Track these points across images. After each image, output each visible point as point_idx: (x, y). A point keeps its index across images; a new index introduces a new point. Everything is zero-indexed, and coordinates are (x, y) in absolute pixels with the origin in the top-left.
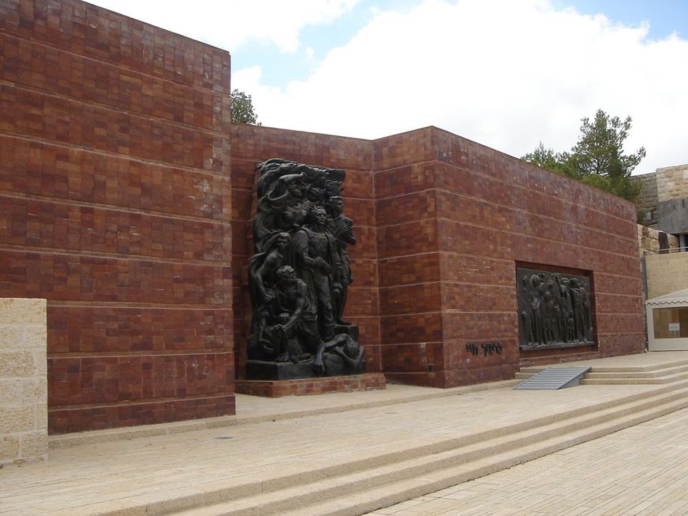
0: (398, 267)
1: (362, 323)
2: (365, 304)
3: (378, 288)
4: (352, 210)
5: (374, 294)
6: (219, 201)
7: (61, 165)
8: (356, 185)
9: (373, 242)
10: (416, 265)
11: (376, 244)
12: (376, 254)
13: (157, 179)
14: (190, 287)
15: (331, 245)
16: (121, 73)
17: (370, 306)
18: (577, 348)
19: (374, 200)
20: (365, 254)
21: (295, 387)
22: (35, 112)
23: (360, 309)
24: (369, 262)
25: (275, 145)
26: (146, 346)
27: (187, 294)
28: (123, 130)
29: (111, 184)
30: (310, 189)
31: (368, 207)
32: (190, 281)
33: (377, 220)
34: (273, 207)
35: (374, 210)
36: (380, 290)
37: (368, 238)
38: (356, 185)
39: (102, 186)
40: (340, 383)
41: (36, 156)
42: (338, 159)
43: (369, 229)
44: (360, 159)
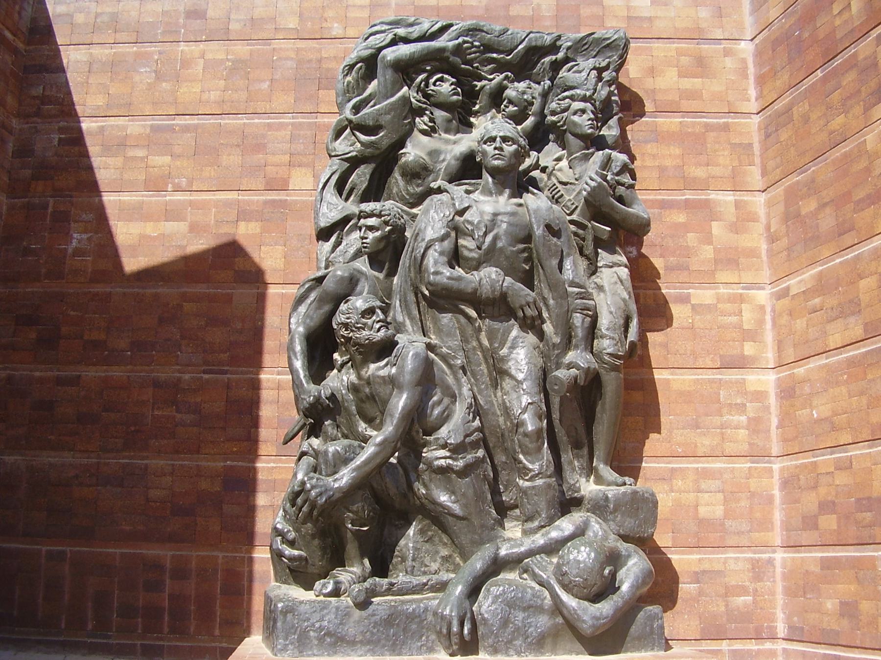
0: (817, 301)
1: (714, 484)
2: (722, 427)
3: (771, 378)
4: (678, 151)
5: (760, 396)
8: (688, 83)
9: (755, 239)
10: (863, 283)
11: (764, 247)
12: (765, 275)
15: (539, 231)
17: (743, 433)
19: (756, 119)
20: (723, 276)
23: (705, 443)
24: (741, 299)
30: (501, 89)
31: (737, 141)
33: (764, 173)
34: (363, 137)
35: (757, 148)
36: (779, 382)
37: (736, 228)
38: (688, 83)
42: (629, 18)
43: (738, 204)
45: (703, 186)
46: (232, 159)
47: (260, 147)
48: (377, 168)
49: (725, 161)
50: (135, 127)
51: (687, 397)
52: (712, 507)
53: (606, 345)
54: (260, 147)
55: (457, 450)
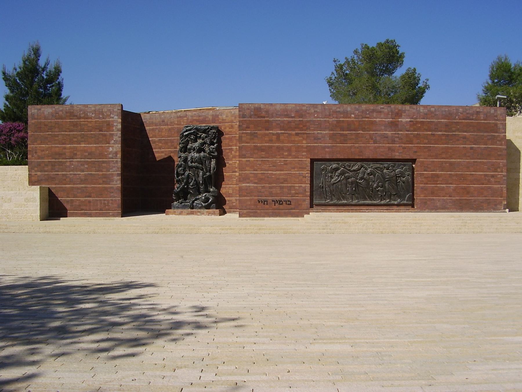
6: (116, 153)
7: (64, 151)
8: (230, 130)
13: (93, 150)
14: (104, 180)
16: (81, 121)
18: (398, 205)
21: (175, 212)
22: (56, 138)
25: (195, 118)
26: (90, 197)
27: (103, 181)
28: (82, 138)
29: (78, 153)
32: (105, 178)
37: (235, 152)
38: (230, 130)
39: (76, 154)
40: (196, 212)
41: (57, 149)
44: (233, 118)
45: (231, 146)
46: (170, 144)
47: (173, 142)
48: (185, 149)
49: (235, 142)
50: (157, 139)
51: (228, 176)
52: (231, 191)
53: (212, 172)
54: (173, 142)
55: (192, 186)
